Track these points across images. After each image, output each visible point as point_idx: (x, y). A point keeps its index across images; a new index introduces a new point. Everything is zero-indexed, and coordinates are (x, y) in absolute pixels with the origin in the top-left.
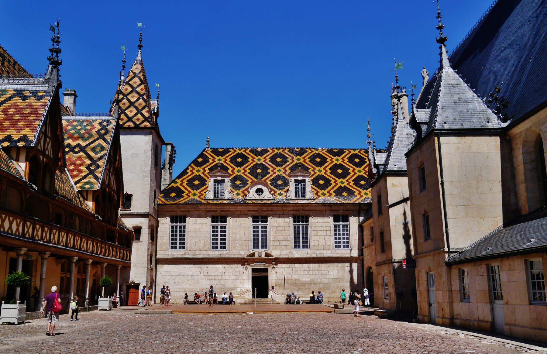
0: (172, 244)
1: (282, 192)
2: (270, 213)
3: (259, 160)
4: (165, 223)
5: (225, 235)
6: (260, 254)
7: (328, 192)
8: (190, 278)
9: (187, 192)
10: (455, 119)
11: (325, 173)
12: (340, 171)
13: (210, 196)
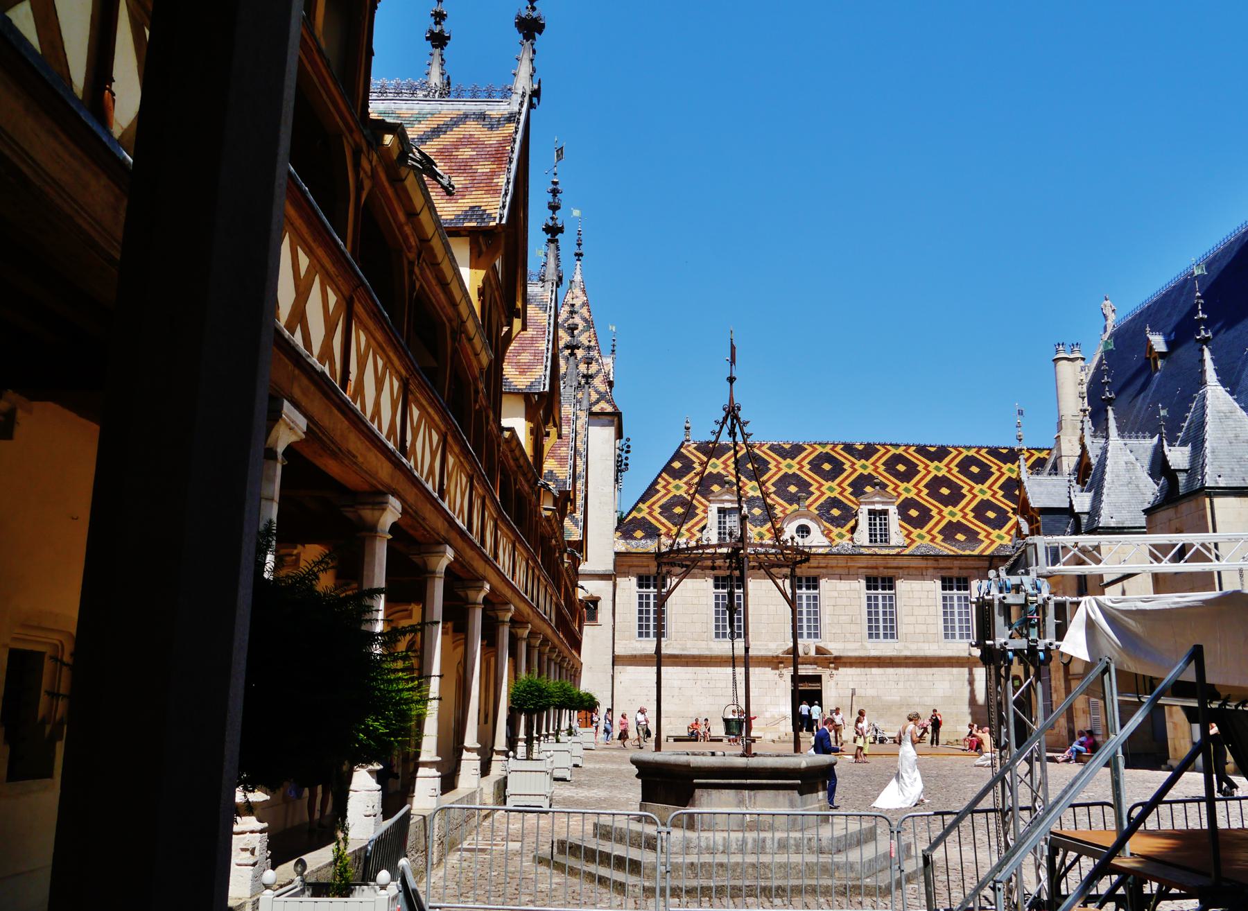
0: (640, 627)
1: (843, 531)
2: (824, 571)
4: (629, 586)
10: (1232, 470)
11: (917, 494)
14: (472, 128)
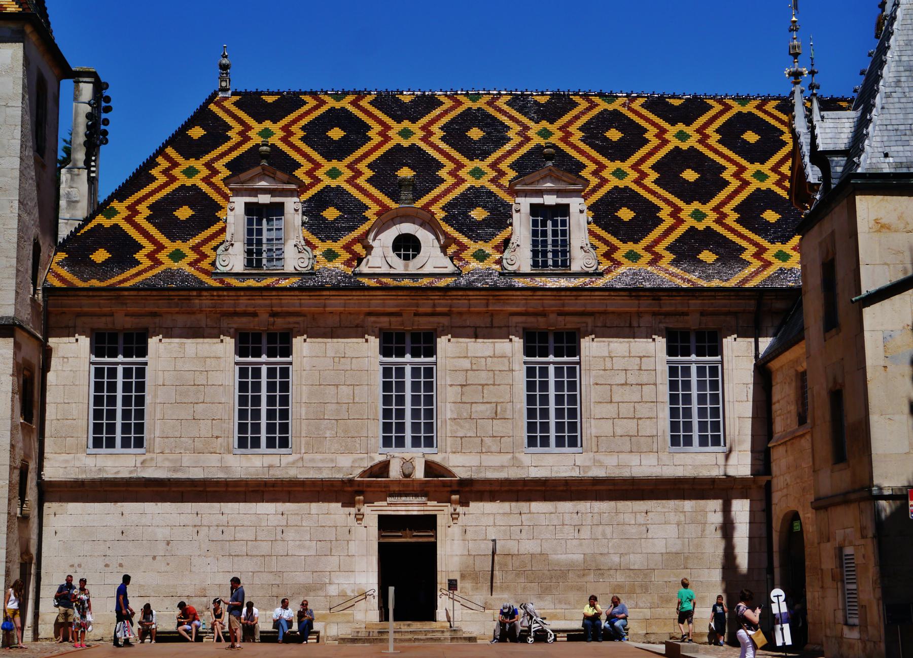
0: (97, 428)
1: (488, 248)
2: (444, 320)
3: (406, 134)
4: (72, 357)
5: (285, 401)
6: (408, 463)
7: (648, 249)
8: (161, 549)
9: (149, 247)
11: (637, 182)
12: (690, 175)
13: (234, 260)
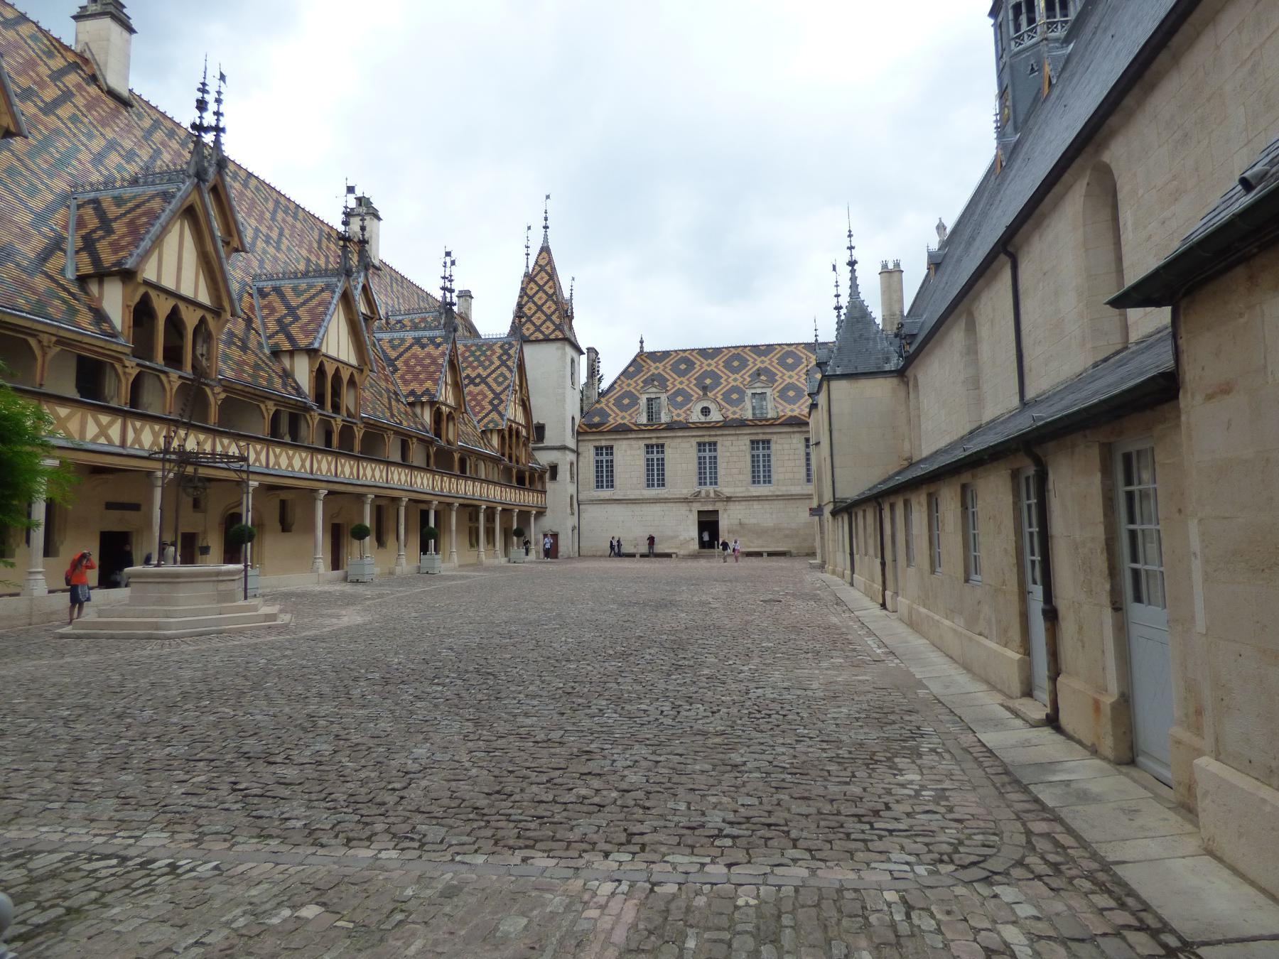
14: (156, 204)
